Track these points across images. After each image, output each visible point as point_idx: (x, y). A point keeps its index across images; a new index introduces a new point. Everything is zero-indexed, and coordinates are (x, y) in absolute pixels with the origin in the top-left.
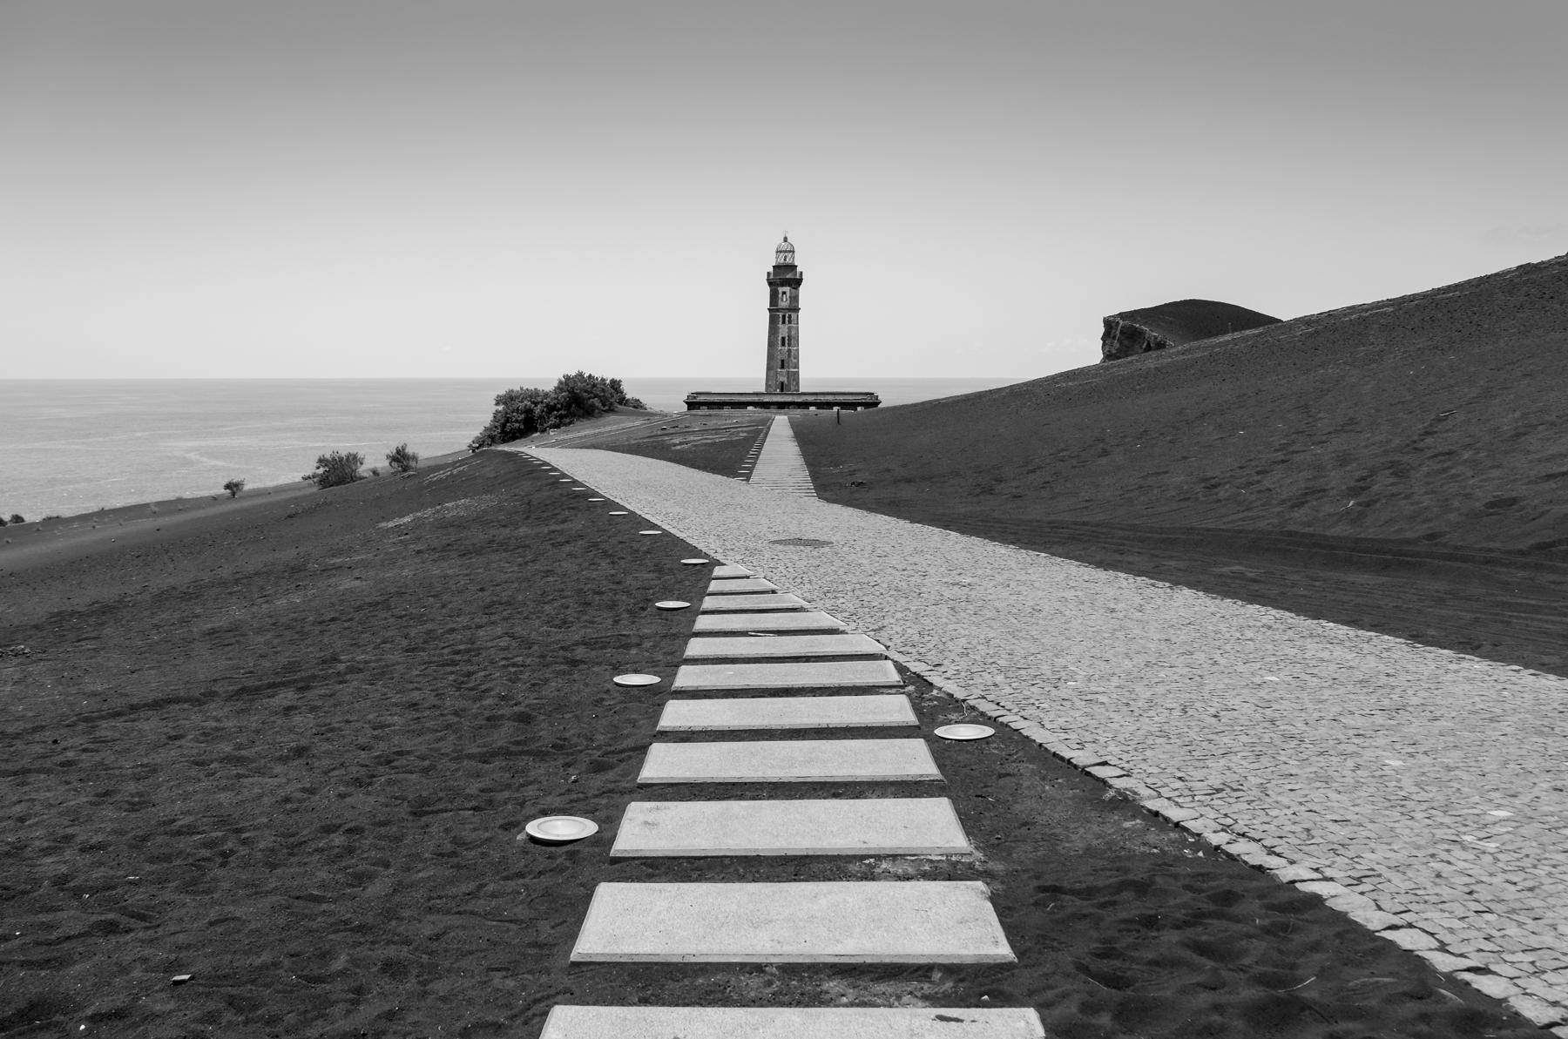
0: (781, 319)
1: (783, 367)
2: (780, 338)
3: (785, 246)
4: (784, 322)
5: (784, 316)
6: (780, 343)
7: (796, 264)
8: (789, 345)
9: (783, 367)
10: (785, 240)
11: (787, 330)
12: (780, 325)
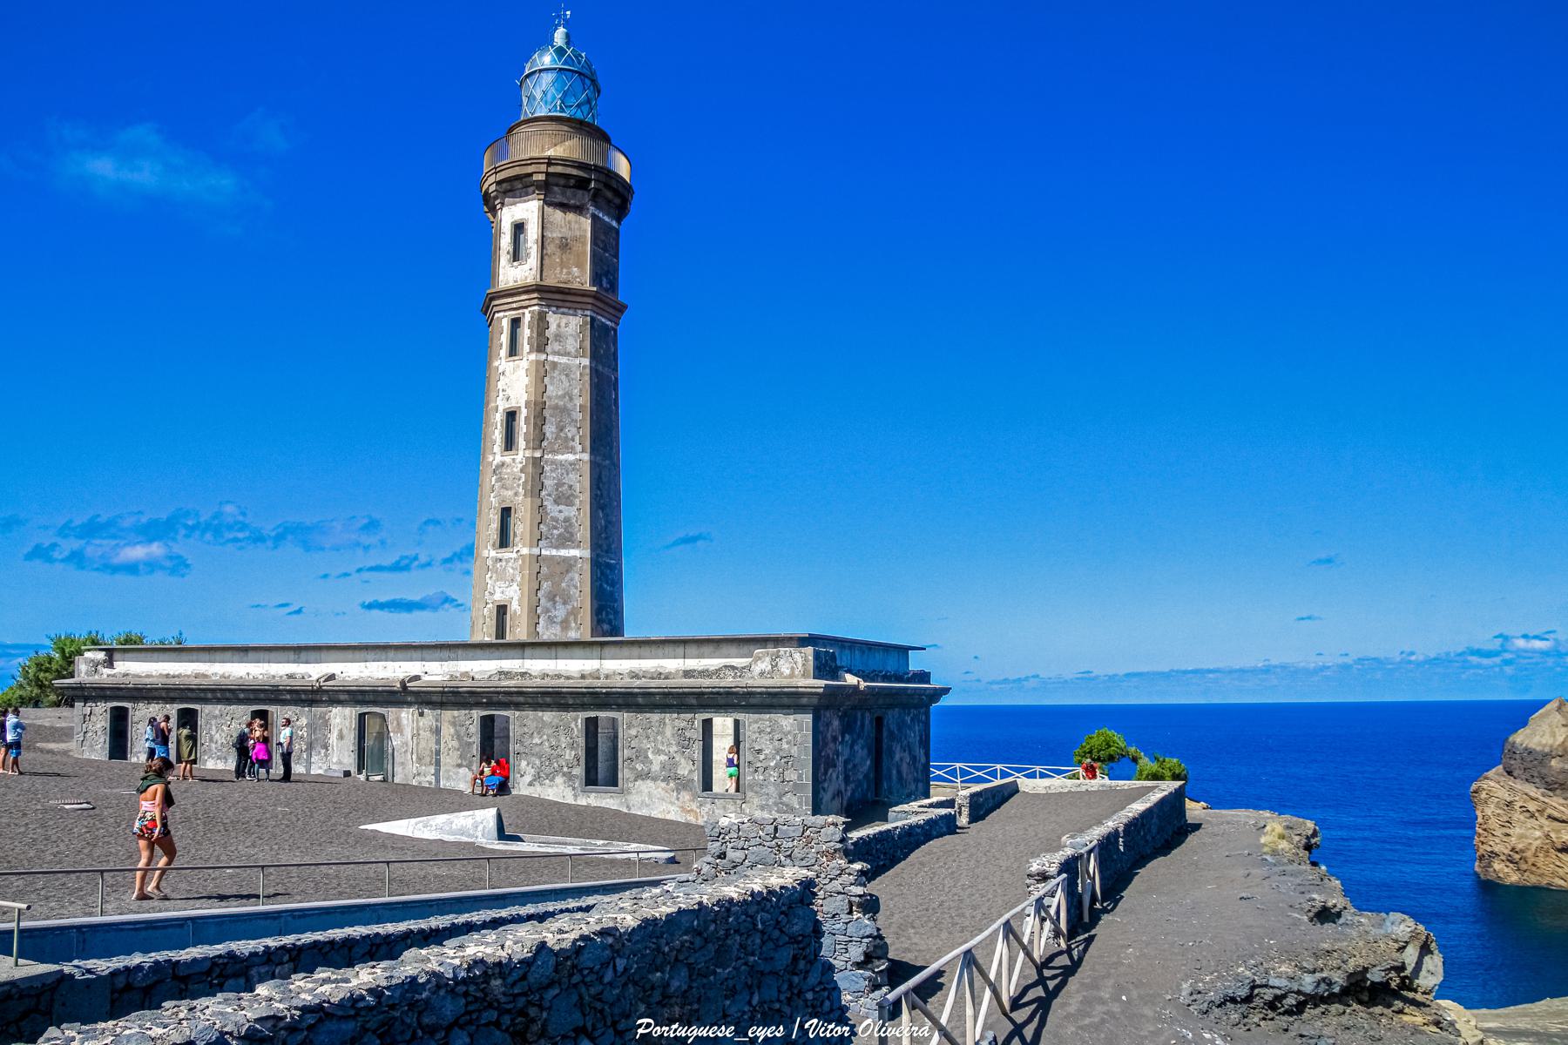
0: (505, 339)
2: (499, 418)
4: (513, 351)
5: (516, 323)
6: (498, 435)
8: (538, 440)
9: (504, 541)
11: (526, 380)
12: (502, 362)
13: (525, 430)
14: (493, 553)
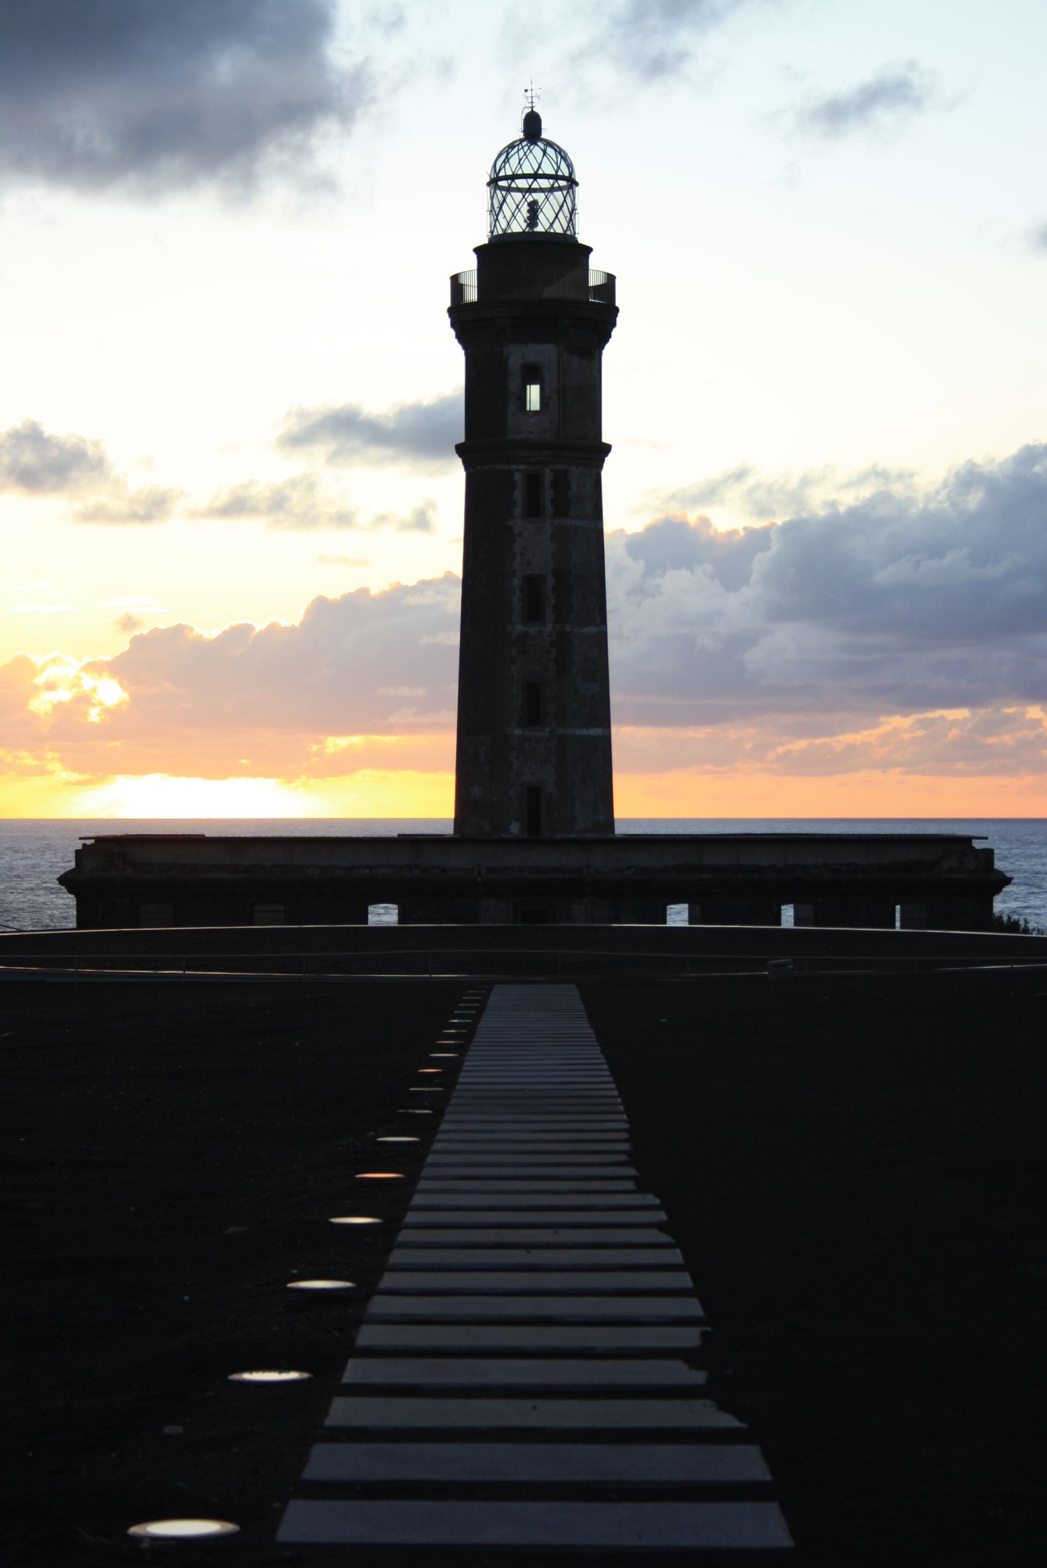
0: (518, 494)
1: (533, 717)
2: (516, 582)
3: (533, 159)
4: (533, 510)
5: (534, 482)
6: (516, 602)
7: (582, 239)
9: (533, 717)
10: (532, 126)
12: (517, 523)
13: (553, 602)
14: (518, 732)
